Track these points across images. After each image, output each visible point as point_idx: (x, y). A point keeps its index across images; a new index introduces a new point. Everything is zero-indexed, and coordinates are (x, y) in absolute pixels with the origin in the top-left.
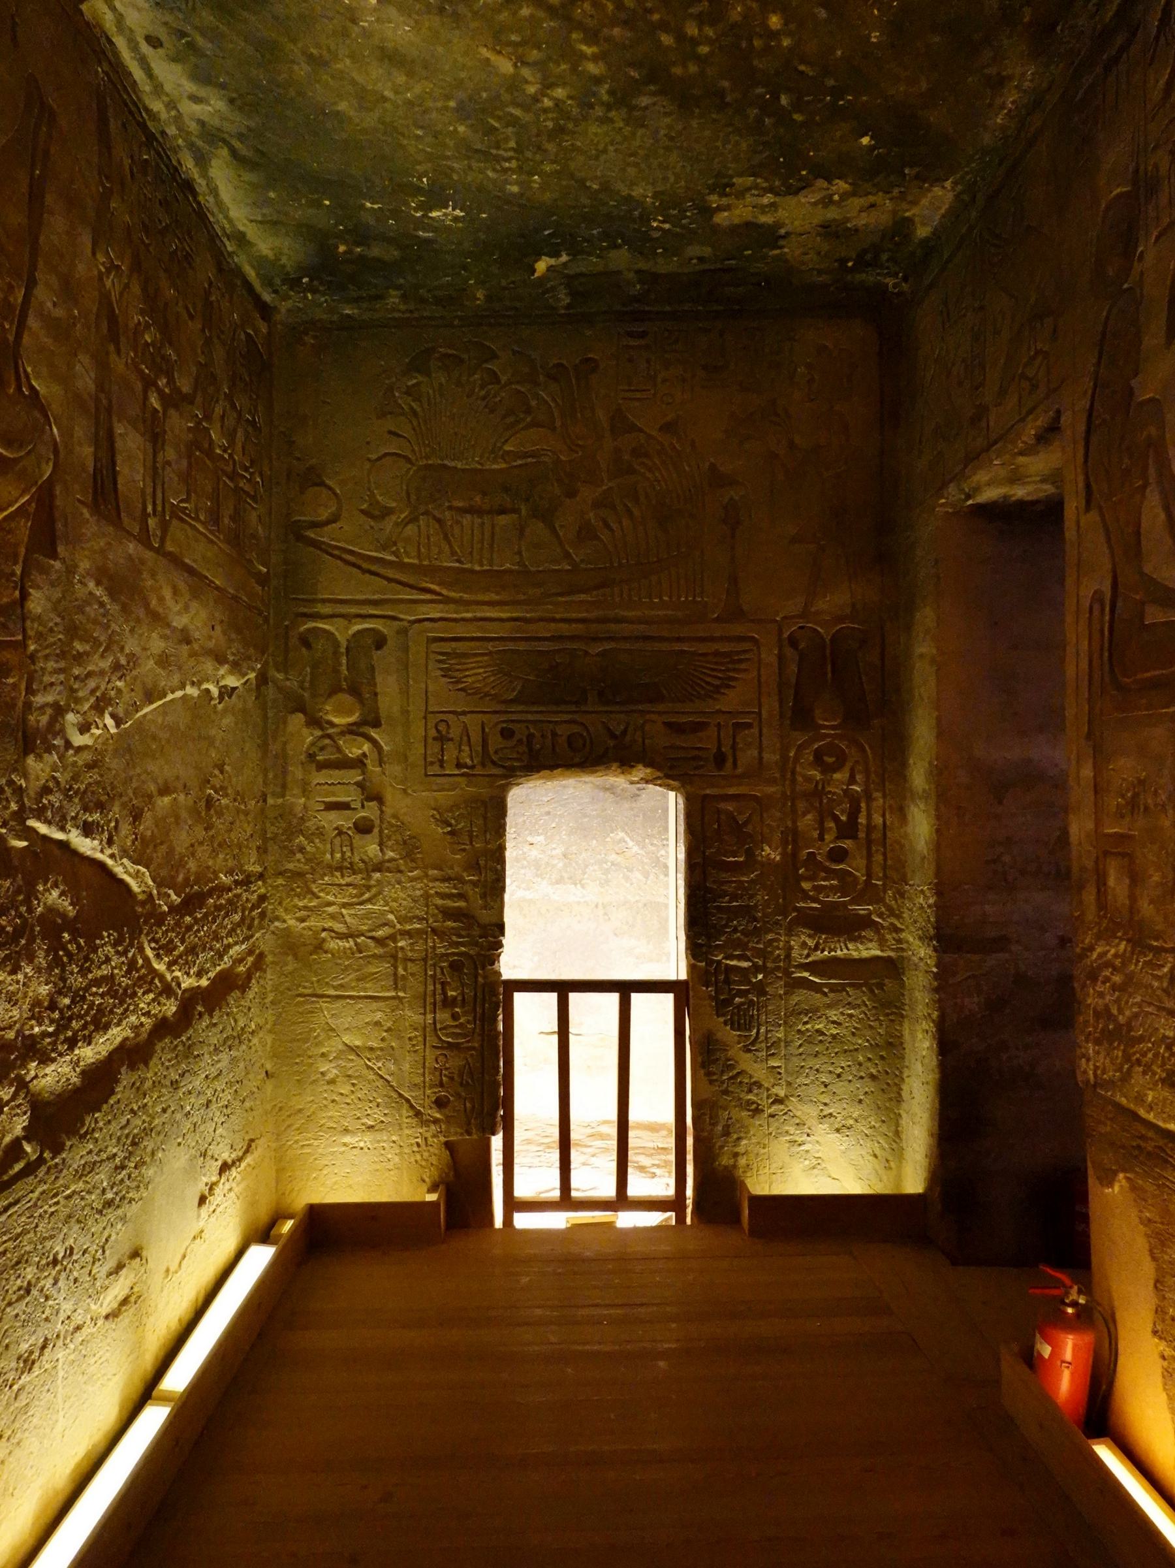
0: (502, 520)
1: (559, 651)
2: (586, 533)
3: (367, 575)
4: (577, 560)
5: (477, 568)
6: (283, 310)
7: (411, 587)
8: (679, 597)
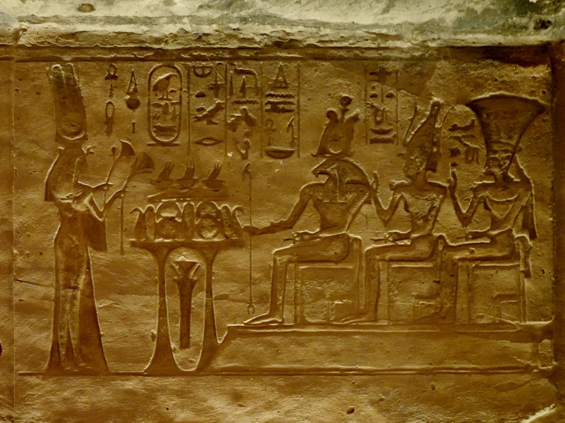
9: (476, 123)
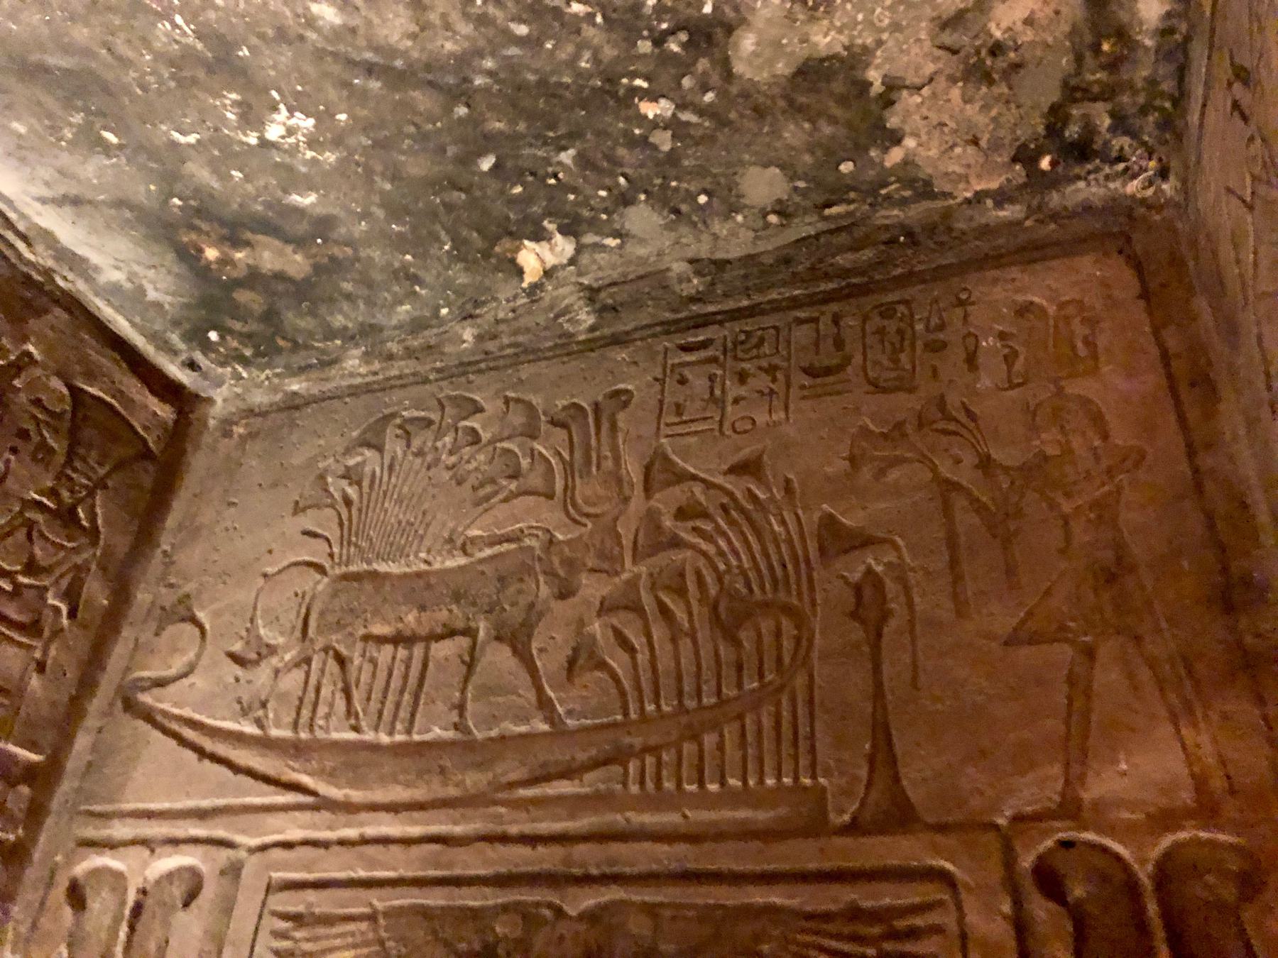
0: (444, 650)
1: (505, 908)
2: (581, 659)
3: (207, 762)
4: (560, 710)
5: (384, 739)
6: (219, 401)
7: (267, 780)
8: (761, 781)
9: (68, 416)
